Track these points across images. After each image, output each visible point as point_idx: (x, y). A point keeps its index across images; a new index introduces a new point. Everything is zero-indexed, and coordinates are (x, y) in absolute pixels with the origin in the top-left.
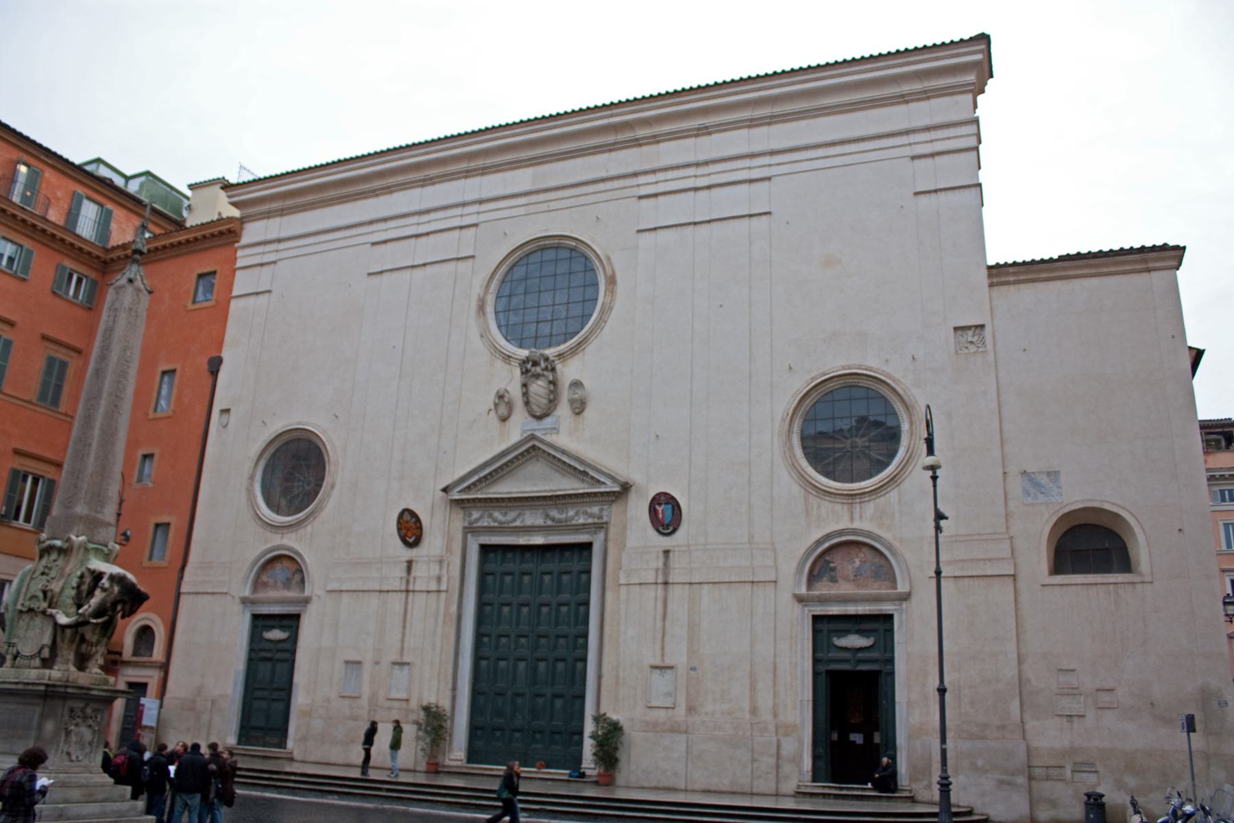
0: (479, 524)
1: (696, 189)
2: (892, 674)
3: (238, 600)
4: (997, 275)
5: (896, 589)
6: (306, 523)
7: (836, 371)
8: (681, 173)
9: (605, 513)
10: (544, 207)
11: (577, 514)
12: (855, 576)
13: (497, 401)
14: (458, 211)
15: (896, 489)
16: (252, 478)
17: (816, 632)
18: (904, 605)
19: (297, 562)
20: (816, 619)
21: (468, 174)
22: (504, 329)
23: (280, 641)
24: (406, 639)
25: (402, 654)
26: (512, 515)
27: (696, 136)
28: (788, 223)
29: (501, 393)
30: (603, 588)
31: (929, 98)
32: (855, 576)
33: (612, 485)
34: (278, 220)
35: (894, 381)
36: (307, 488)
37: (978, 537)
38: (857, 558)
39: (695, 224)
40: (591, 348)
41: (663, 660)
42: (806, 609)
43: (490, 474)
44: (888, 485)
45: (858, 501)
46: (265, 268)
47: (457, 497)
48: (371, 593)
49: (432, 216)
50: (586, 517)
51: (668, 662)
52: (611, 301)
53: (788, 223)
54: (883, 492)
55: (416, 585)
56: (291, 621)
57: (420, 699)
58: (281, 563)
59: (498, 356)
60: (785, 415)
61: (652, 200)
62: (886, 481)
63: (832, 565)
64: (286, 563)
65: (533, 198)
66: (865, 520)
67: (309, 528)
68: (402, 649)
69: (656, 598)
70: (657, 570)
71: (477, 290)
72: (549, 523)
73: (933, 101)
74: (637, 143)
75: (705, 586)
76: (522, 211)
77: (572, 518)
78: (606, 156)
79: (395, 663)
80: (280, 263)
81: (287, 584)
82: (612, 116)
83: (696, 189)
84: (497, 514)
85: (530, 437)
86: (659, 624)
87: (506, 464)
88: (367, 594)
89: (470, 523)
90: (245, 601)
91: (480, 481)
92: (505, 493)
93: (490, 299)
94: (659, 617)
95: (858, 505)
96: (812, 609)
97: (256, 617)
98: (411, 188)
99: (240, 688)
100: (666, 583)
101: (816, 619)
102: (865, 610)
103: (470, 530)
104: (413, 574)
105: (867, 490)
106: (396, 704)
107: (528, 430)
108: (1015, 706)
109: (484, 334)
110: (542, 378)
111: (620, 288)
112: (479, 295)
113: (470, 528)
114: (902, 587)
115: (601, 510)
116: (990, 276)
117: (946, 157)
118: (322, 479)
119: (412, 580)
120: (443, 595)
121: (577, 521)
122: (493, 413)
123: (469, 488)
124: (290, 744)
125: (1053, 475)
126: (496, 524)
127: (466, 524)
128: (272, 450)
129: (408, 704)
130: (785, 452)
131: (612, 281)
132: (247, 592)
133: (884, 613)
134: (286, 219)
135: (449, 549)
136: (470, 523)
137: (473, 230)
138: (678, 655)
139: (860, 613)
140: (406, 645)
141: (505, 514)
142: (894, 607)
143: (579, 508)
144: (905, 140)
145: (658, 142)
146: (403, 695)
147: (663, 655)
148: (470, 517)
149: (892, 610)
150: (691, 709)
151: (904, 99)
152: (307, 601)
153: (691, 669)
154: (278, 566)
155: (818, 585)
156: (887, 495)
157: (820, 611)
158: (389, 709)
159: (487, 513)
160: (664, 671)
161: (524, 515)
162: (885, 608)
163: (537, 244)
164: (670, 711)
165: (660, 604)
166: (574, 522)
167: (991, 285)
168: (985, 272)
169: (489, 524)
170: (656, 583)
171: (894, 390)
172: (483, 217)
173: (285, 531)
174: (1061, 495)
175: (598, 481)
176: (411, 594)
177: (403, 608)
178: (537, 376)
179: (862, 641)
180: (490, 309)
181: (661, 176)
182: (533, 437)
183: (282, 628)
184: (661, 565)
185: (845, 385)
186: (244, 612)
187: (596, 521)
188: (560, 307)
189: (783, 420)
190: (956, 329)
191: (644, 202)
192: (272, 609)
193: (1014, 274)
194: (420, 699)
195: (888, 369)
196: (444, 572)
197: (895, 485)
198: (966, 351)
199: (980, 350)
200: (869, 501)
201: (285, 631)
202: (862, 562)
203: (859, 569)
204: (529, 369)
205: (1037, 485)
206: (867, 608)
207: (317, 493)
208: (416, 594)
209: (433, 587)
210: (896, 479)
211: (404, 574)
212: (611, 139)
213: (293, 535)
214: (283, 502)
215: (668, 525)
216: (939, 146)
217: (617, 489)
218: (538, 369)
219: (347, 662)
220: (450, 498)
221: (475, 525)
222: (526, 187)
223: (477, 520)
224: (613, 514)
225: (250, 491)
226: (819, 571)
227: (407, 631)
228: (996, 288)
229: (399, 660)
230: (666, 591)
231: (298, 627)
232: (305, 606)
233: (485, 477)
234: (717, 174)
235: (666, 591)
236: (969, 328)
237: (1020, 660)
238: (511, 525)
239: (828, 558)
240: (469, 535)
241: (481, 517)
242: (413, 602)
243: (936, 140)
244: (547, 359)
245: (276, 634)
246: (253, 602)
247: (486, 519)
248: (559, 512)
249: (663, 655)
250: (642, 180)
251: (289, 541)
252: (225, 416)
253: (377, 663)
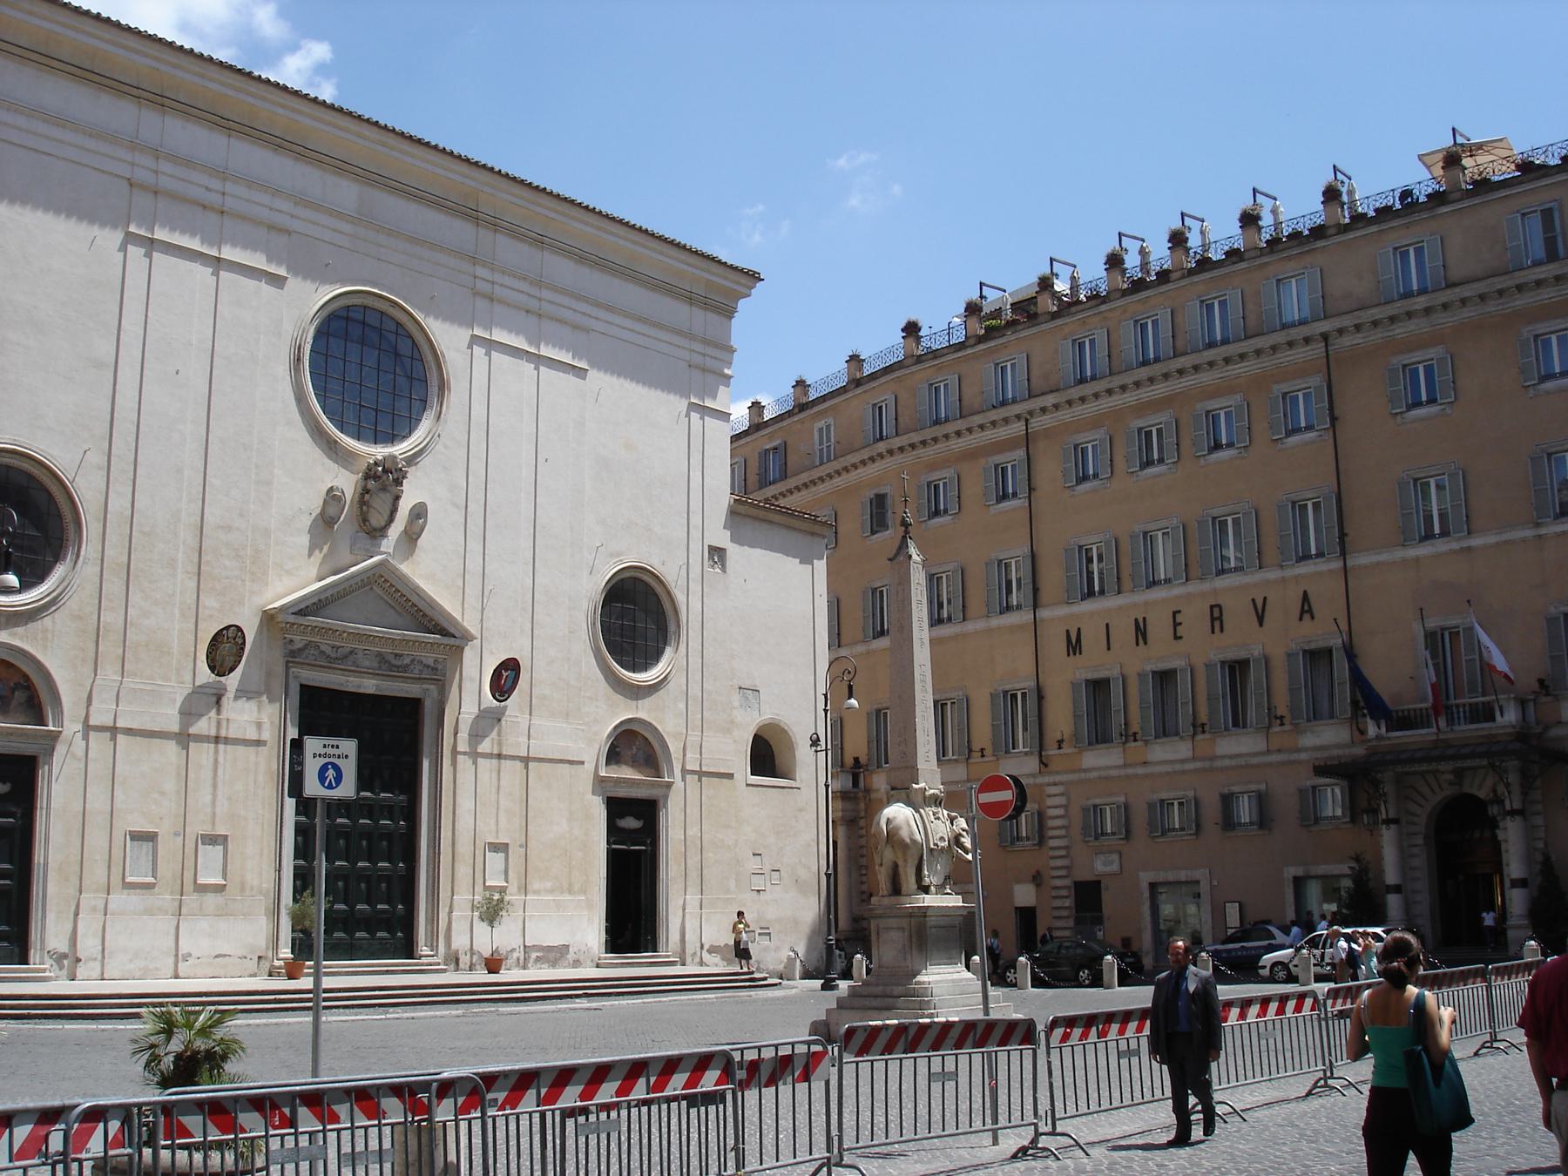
24: (218, 804)
25: (214, 824)
55: (231, 730)
66: (642, 711)
67: (47, 621)
86: (494, 797)
89: (293, 654)
94: (494, 790)
109: (300, 398)
119: (224, 723)
131: (443, 386)
140: (218, 810)
165: (494, 775)
171: (669, 593)
172: (297, 225)
177: (211, 760)
203: (635, 755)
213: (20, 630)
215: (506, 692)
241: (306, 647)
253: (177, 834)
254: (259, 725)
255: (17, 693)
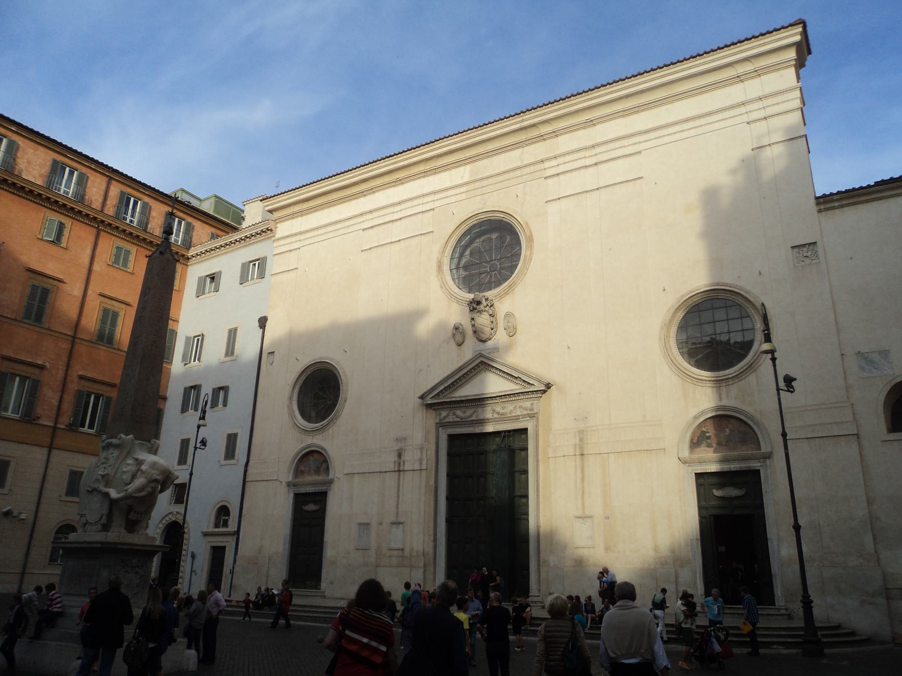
0: (447, 420)
1: (586, 167)
2: (763, 516)
3: (284, 484)
4: (824, 202)
5: (760, 450)
6: (328, 428)
7: (700, 289)
8: (575, 156)
9: (535, 406)
10: (479, 192)
11: (515, 407)
12: (726, 442)
13: (454, 332)
14: (420, 201)
15: (754, 374)
16: (291, 398)
17: (699, 486)
18: (768, 462)
19: (323, 454)
20: (698, 476)
21: (425, 174)
22: (457, 281)
23: (314, 511)
24: (400, 506)
25: (397, 517)
26: (469, 412)
27: (584, 128)
28: (656, 183)
29: (457, 326)
30: (537, 461)
31: (759, 75)
32: (726, 442)
33: (540, 386)
34: (299, 219)
35: (746, 292)
36: (329, 402)
37: (823, 406)
38: (727, 428)
39: (587, 192)
40: (518, 289)
41: (584, 512)
42: (690, 469)
43: (452, 384)
44: (747, 371)
45: (724, 384)
46: (293, 253)
47: (429, 402)
48: (375, 474)
49: (403, 206)
50: (522, 410)
51: (588, 513)
52: (531, 254)
53: (656, 183)
54: (744, 377)
56: (321, 498)
57: (412, 550)
58: (313, 456)
59: (453, 300)
60: (664, 324)
61: (556, 179)
62: (745, 368)
63: (707, 434)
64: (316, 456)
65: (472, 186)
67: (330, 431)
68: (398, 513)
69: (576, 466)
70: (575, 445)
71: (435, 255)
72: (496, 416)
73: (764, 78)
74: (542, 138)
75: (612, 455)
76: (464, 196)
77: (511, 412)
78: (520, 151)
79: (393, 523)
80: (301, 248)
81: (317, 471)
82: (523, 121)
83: (586, 167)
84: (459, 412)
85: (479, 355)
87: (463, 376)
88: (372, 474)
90: (289, 484)
91: (445, 389)
92: (463, 397)
93: (446, 261)
94: (579, 481)
95: (724, 388)
96: (694, 468)
97: (297, 496)
98: (387, 188)
99: (287, 546)
100: (582, 455)
101: (698, 476)
102: (737, 467)
103: (441, 425)
104: (403, 458)
105: (731, 376)
106: (395, 553)
107: (477, 351)
108: (868, 539)
109: (443, 285)
110: (483, 313)
111: (536, 245)
112: (438, 258)
113: (440, 423)
114: (764, 449)
115: (532, 404)
116: (818, 204)
117: (777, 118)
118: (338, 396)
119: (402, 463)
120: (424, 473)
121: (515, 413)
122: (452, 340)
123: (438, 394)
124: (323, 585)
125: (884, 353)
126: (459, 420)
127: (438, 421)
128: (303, 377)
129: (403, 553)
130: (665, 353)
131: (530, 239)
132: (290, 479)
133: (752, 469)
134: (305, 218)
135: (426, 439)
136: (440, 420)
137: (431, 213)
138: (596, 507)
139: (733, 470)
140: (400, 509)
141: (465, 412)
142: (759, 464)
143: (515, 404)
144: (743, 109)
145: (557, 136)
146: (400, 546)
147: (583, 509)
148: (440, 416)
149: (759, 466)
150: (607, 549)
151: (739, 79)
152: (331, 482)
153: (605, 518)
154: (311, 458)
155: (698, 450)
156: (747, 379)
157: (701, 469)
158: (391, 557)
159: (451, 412)
160: (585, 520)
161: (477, 412)
162: (752, 465)
163: (477, 218)
164: (592, 550)
165: (579, 470)
166: (513, 414)
167: (820, 211)
168: (813, 201)
169: (454, 419)
170: (576, 455)
172: (437, 204)
173: (314, 434)
174: (893, 369)
175: (529, 383)
176: (402, 473)
177: (396, 484)
178: (480, 312)
179: (736, 491)
180: (446, 268)
181: (560, 160)
182: (481, 355)
183: (315, 502)
184: (577, 441)
185: (708, 298)
186: (289, 491)
187: (529, 412)
188: (496, 262)
189: (662, 328)
190: (792, 247)
191: (550, 181)
192: (308, 489)
193: (838, 200)
194: (412, 550)
195: (740, 283)
196: (424, 456)
197: (752, 370)
198: (803, 263)
199: (814, 261)
200: (733, 384)
201: (317, 505)
202: (732, 431)
204: (474, 306)
205: (871, 362)
206: (738, 466)
207: (335, 406)
208: (406, 472)
209: (417, 467)
210: (752, 366)
211: (396, 459)
212: (522, 136)
214: (313, 414)
216: (770, 111)
217: (543, 388)
218: (481, 307)
219: (360, 524)
220: (425, 403)
221: (444, 421)
222: (466, 179)
223: (445, 418)
224: (539, 405)
225: (290, 407)
226: (698, 440)
227: (401, 499)
228: (823, 213)
229: (396, 521)
230: (583, 460)
231: (326, 501)
232: (330, 486)
233: (449, 386)
234: (603, 153)
235: (583, 460)
236: (804, 245)
237: (870, 502)
238: (469, 419)
239: (704, 429)
240: (440, 428)
241: (448, 415)
242: (404, 479)
243: (768, 106)
244: (487, 299)
245: (311, 507)
246: (295, 485)
247: (451, 416)
248: (502, 407)
249: (583, 509)
250: (547, 164)
251: (318, 441)
252: (271, 356)
253: (381, 524)
254: (421, 460)
255: (323, 465)
